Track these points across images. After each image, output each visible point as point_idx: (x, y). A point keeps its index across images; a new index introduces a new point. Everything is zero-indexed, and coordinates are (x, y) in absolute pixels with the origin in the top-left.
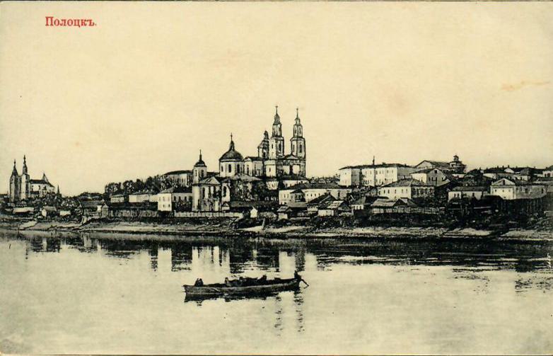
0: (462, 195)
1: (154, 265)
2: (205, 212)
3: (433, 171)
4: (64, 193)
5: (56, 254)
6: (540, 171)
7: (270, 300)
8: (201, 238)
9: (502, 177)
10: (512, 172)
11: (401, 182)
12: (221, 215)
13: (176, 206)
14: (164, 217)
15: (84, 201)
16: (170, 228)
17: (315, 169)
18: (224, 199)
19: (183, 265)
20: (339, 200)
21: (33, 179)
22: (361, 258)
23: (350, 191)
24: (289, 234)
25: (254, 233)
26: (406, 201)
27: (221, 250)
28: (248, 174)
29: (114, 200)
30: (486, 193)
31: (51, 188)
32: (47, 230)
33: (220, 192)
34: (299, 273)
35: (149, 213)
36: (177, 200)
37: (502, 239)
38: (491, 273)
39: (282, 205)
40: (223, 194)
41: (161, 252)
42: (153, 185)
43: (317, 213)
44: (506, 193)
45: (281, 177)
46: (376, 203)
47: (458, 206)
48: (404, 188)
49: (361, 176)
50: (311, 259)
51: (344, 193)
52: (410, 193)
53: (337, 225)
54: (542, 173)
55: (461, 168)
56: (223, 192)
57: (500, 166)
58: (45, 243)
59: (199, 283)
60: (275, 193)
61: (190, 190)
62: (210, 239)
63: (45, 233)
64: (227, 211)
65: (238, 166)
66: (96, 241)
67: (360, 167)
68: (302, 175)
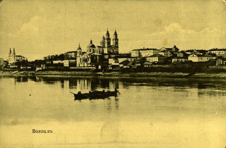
0: (177, 60)
1: (63, 86)
2: (81, 67)
3: (166, 52)
4: (29, 61)
5: (26, 83)
6: (207, 51)
7: (106, 100)
8: (80, 77)
9: (192, 54)
10: (196, 51)
11: (154, 56)
12: (88, 68)
13: (71, 64)
14: (67, 69)
15: (38, 63)
16: (69, 73)
17: (122, 50)
18: (88, 62)
19: (74, 87)
20: (131, 62)
21: (17, 55)
22: (140, 84)
23: (135, 59)
24: (113, 75)
25: (99, 74)
26: (156, 63)
27: (87, 81)
28: (97, 53)
29: (47, 62)
30: (186, 60)
31: (24, 59)
32: (23, 74)
33: (87, 59)
34: (117, 90)
35: (60, 68)
36: (71, 62)
37: (193, 77)
38: (188, 89)
39: (110, 64)
40: (88, 60)
41: (65, 81)
42: (62, 57)
43: (123, 67)
44: (194, 59)
45: (109, 53)
46: (146, 63)
47: (176, 64)
48: (156, 58)
49: (139, 53)
51: (133, 60)
52: (157, 59)
53: (131, 72)
54: (208, 52)
55: (177, 50)
56: (88, 59)
57: (192, 50)
58: (22, 79)
59: (79, 93)
60: (107, 60)
61: (75, 59)
62: (84, 77)
63: (22, 75)
64: (90, 67)
65: (94, 49)
66: (41, 78)
67: (139, 50)
68: (117, 53)
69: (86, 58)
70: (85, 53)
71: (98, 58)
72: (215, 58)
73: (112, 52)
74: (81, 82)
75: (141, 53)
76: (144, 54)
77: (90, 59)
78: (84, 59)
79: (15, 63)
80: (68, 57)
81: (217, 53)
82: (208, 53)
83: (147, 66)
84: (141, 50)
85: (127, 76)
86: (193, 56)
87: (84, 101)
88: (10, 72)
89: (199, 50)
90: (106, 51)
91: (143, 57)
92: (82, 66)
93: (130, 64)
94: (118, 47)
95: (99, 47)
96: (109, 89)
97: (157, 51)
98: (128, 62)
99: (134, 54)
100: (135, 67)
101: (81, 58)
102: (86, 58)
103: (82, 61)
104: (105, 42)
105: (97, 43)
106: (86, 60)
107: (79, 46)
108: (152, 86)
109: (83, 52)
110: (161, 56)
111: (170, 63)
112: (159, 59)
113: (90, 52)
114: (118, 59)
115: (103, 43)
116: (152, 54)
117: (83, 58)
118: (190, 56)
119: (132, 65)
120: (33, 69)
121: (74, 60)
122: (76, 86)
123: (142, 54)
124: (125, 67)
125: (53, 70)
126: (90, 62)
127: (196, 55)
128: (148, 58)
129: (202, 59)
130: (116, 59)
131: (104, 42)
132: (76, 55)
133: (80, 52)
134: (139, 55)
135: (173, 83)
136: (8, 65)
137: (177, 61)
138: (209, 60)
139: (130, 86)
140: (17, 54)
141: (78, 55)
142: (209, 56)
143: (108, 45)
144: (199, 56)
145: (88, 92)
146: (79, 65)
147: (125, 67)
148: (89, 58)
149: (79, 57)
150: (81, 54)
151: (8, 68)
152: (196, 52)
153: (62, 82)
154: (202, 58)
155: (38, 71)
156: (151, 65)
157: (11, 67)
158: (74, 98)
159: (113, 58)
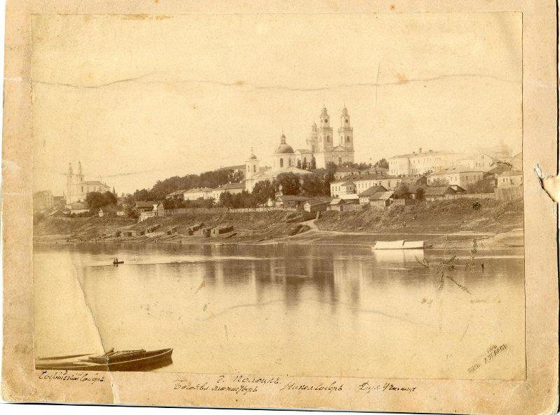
26: (455, 188)
51: (394, 183)
67: (407, 156)
84: (415, 154)
94: (351, 151)
95: (303, 152)
104: (319, 137)
105: (299, 142)
113: (282, 165)
115: (314, 141)
119: (391, 199)
130: (350, 180)
140: (86, 179)
143: (325, 145)
149: (252, 180)
159: (341, 180)
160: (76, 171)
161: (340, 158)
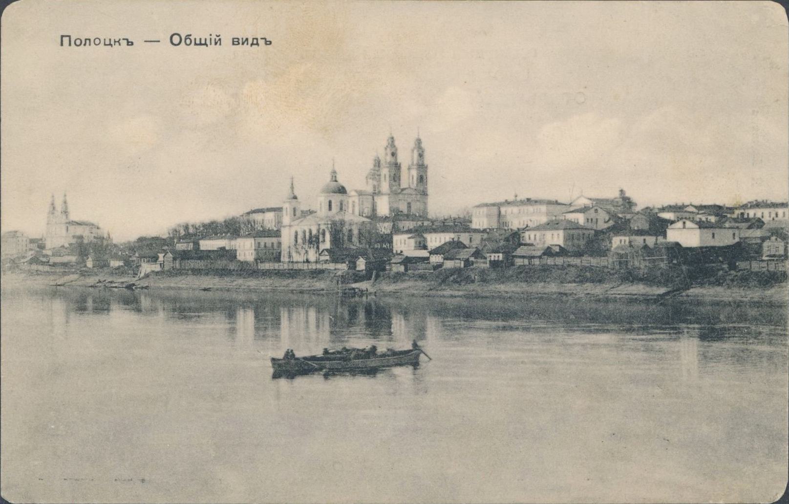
0: (630, 242)
2: (297, 262)
3: (592, 211)
6: (731, 210)
12: (319, 266)
14: (247, 271)
21: (77, 219)
29: (181, 247)
34: (420, 343)
38: (664, 344)
40: (321, 239)
42: (232, 228)
45: (396, 216)
46: (520, 251)
48: (555, 233)
50: (432, 325)
54: (733, 213)
55: (628, 203)
57: (680, 204)
59: (290, 355)
60: (388, 239)
61: (277, 234)
64: (326, 262)
67: (499, 205)
68: (423, 217)
69: (314, 232)
70: (311, 212)
71: (355, 232)
72: (758, 233)
73: (405, 211)
74: (294, 317)
75: (505, 216)
76: (516, 219)
77: (328, 237)
78: (307, 234)
79: (67, 245)
80: (253, 228)
81: (766, 214)
82: (735, 216)
83: (526, 262)
84: (508, 203)
85: (452, 294)
86: (684, 227)
87: (302, 383)
88: (52, 278)
89: (705, 203)
90: (383, 208)
91: (511, 230)
92: (301, 259)
93: (464, 254)
94: (424, 194)
95: (360, 194)
96: (390, 340)
97: (564, 209)
98: (459, 245)
99: (480, 222)
100: (485, 265)
101: (296, 233)
102: (314, 232)
103: (300, 241)
106: (313, 240)
107: (292, 188)
108: (537, 330)
109: (302, 212)
110: (575, 226)
111: (603, 253)
112: (566, 239)
114: (425, 235)
116: (544, 219)
117: (304, 232)
118: (673, 226)
120: (130, 267)
121: (274, 240)
122: (279, 328)
123: (509, 218)
124: (449, 264)
125: (196, 272)
126: (327, 245)
127: (693, 221)
128: (527, 234)
129: (713, 237)
130: (419, 233)
131: (379, 175)
132: (279, 222)
133: (295, 210)
134: (499, 221)
135: (615, 322)
136: (44, 252)
137: (627, 243)
138: (737, 240)
139: (464, 332)
140: (74, 217)
141: (286, 219)
142: (738, 228)
143: (391, 186)
144: (702, 225)
145: (319, 353)
146: (290, 256)
147: (449, 264)
148: (324, 230)
149: (290, 226)
150: (299, 218)
151: (43, 263)
152: (693, 213)
153: (231, 315)
154: (713, 235)
155: (147, 276)
156: (540, 257)
157: (53, 260)
158: (271, 371)
159: (409, 231)
160: (59, 208)
161: (409, 204)
